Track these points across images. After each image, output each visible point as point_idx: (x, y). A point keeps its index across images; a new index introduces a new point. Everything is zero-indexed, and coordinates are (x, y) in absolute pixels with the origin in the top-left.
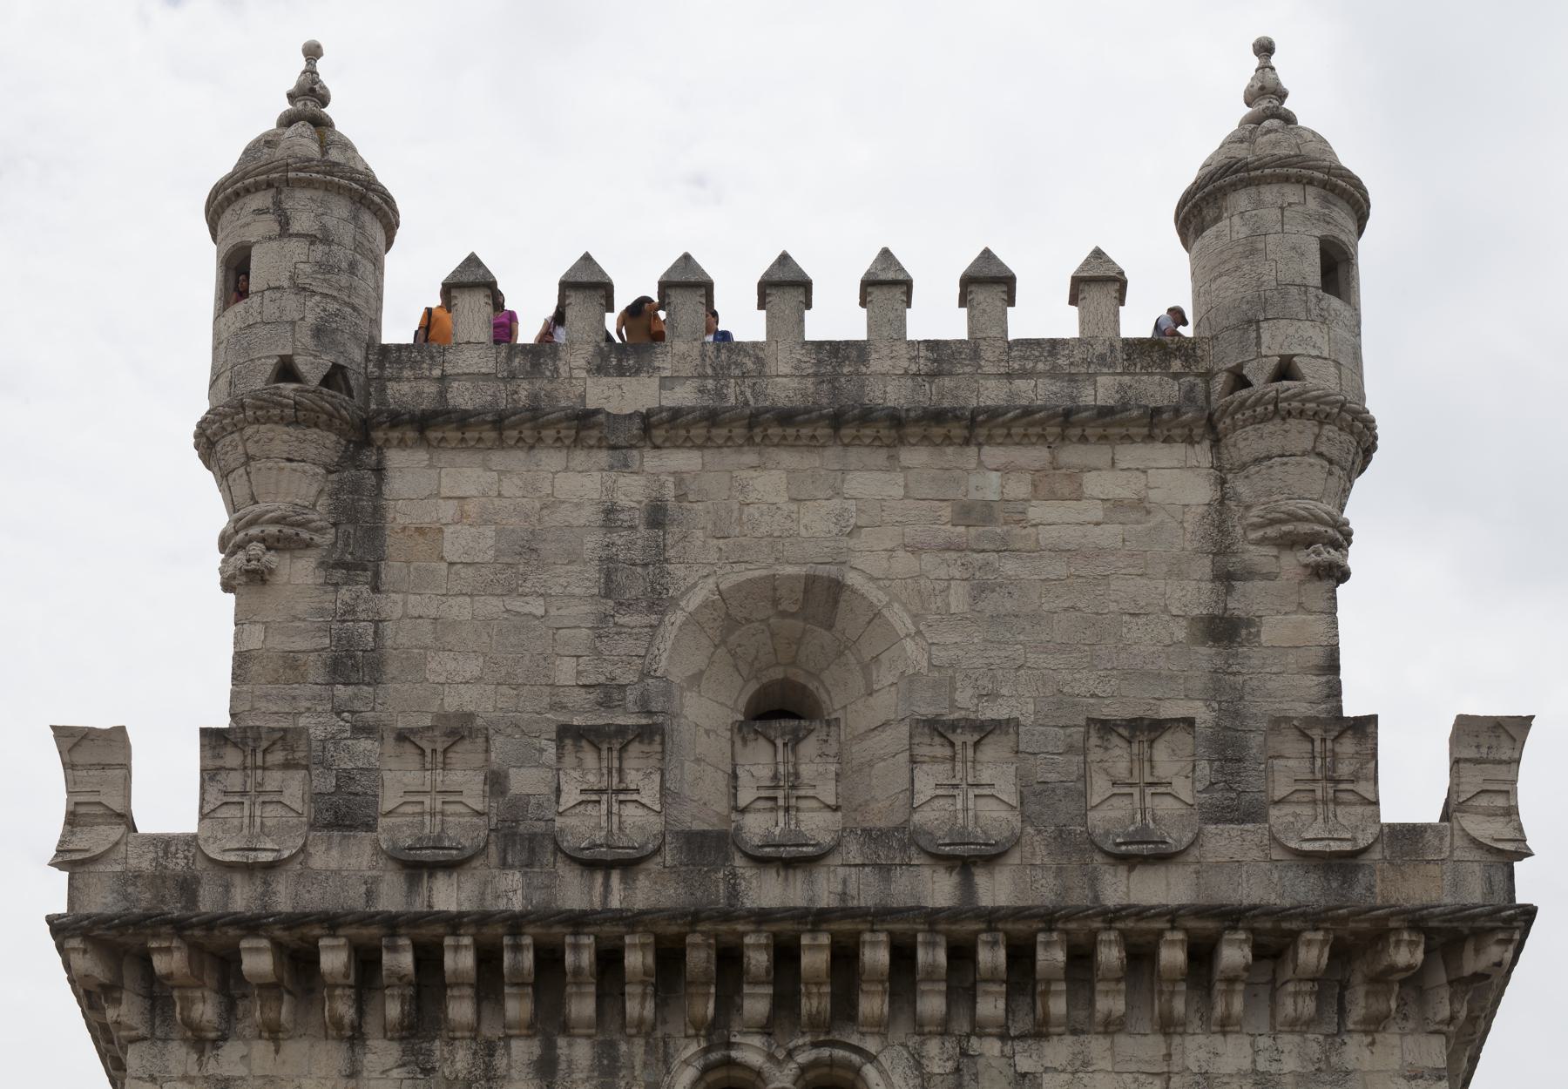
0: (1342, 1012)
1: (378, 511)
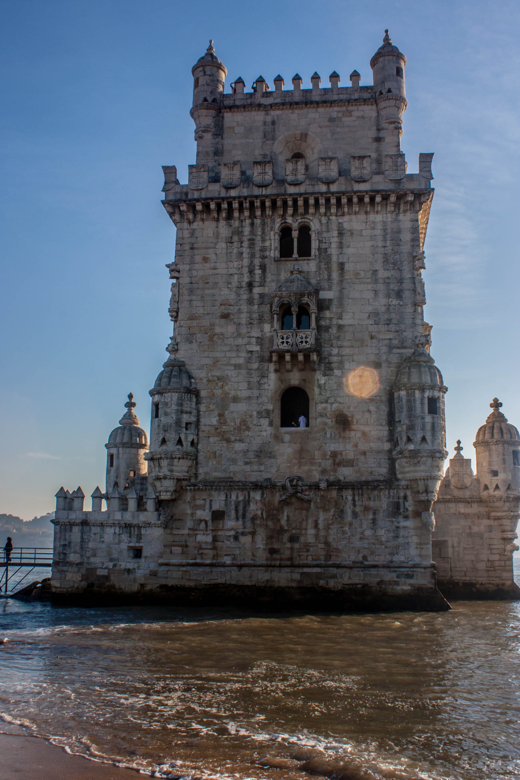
0: (399, 209)
1: (223, 125)
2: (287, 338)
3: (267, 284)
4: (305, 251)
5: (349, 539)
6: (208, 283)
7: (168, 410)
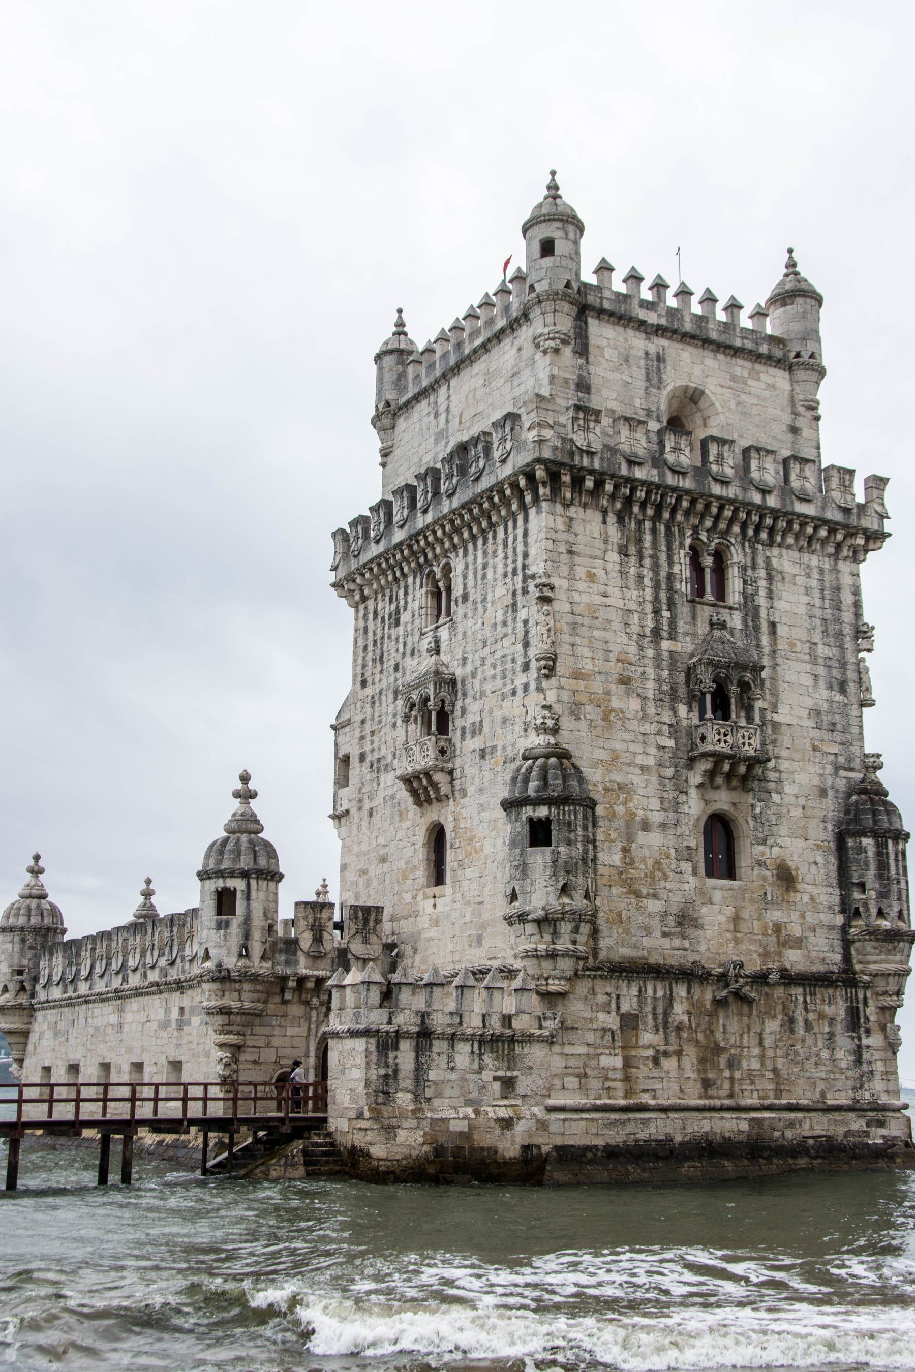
2: (725, 735)
3: (680, 637)
4: (721, 593)
7: (572, 836)
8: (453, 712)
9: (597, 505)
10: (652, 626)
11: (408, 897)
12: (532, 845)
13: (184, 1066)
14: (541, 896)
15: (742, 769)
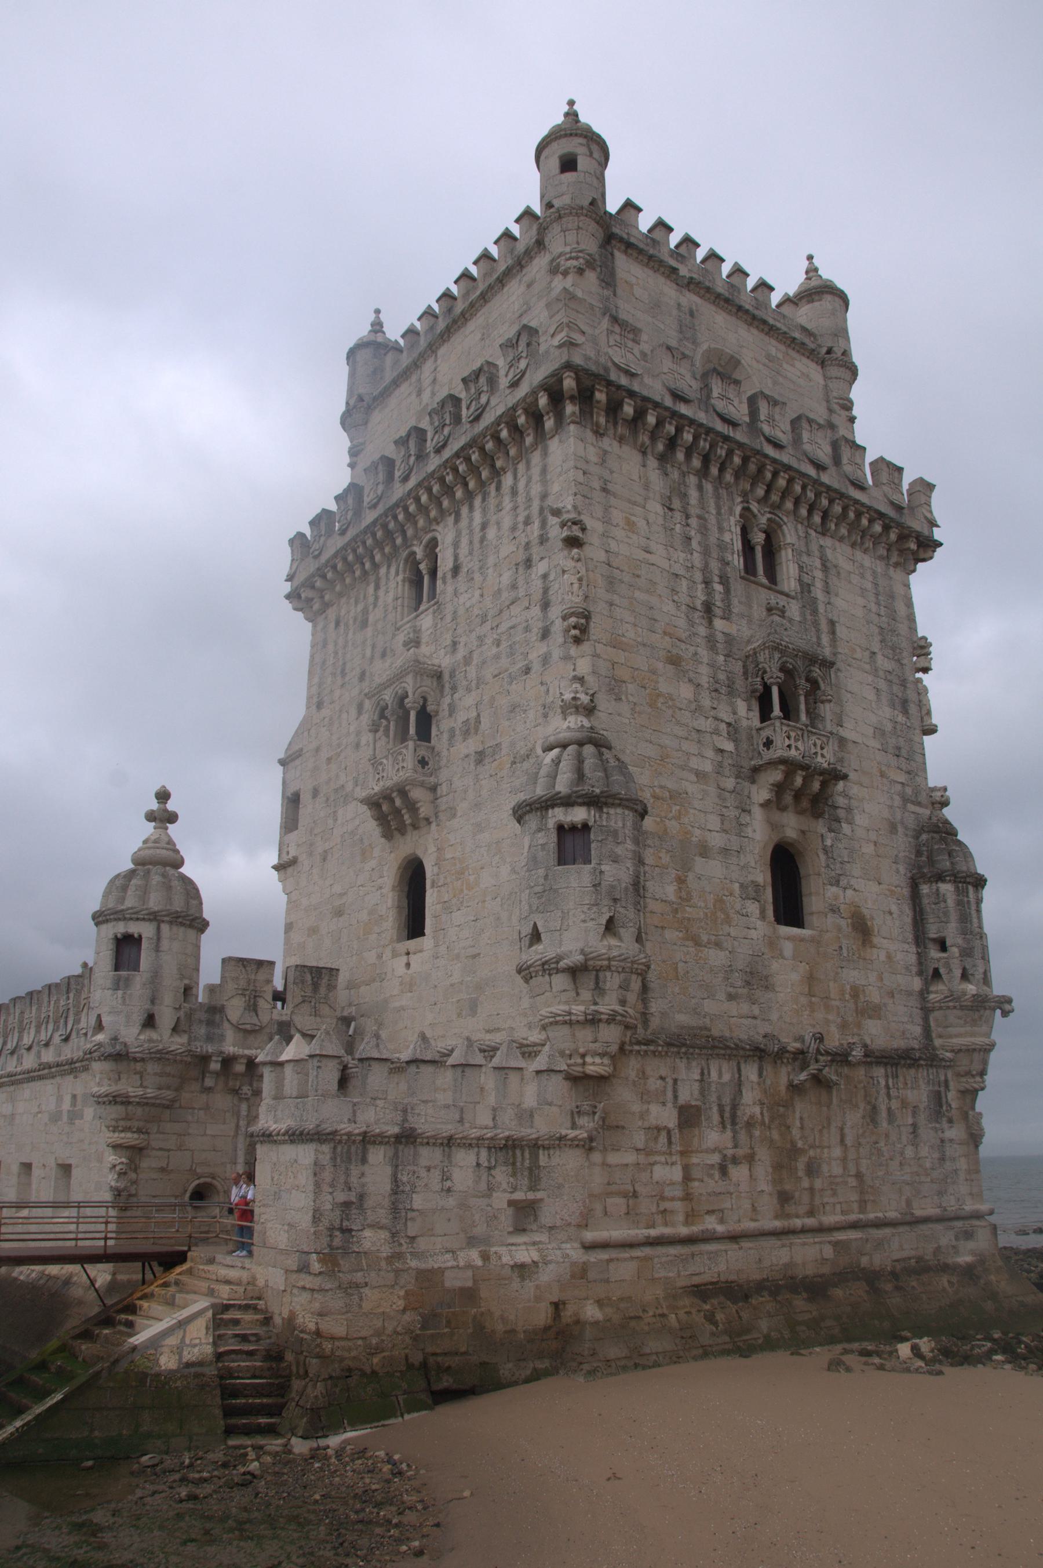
1: (613, 268)
2: (796, 740)
3: (734, 618)
5: (887, 1165)
6: (638, 576)
7: (619, 850)
8: (437, 712)
9: (635, 442)
10: (703, 598)
11: (371, 957)
12: (561, 861)
13: (75, 1172)
14: (575, 936)
15: (816, 786)
